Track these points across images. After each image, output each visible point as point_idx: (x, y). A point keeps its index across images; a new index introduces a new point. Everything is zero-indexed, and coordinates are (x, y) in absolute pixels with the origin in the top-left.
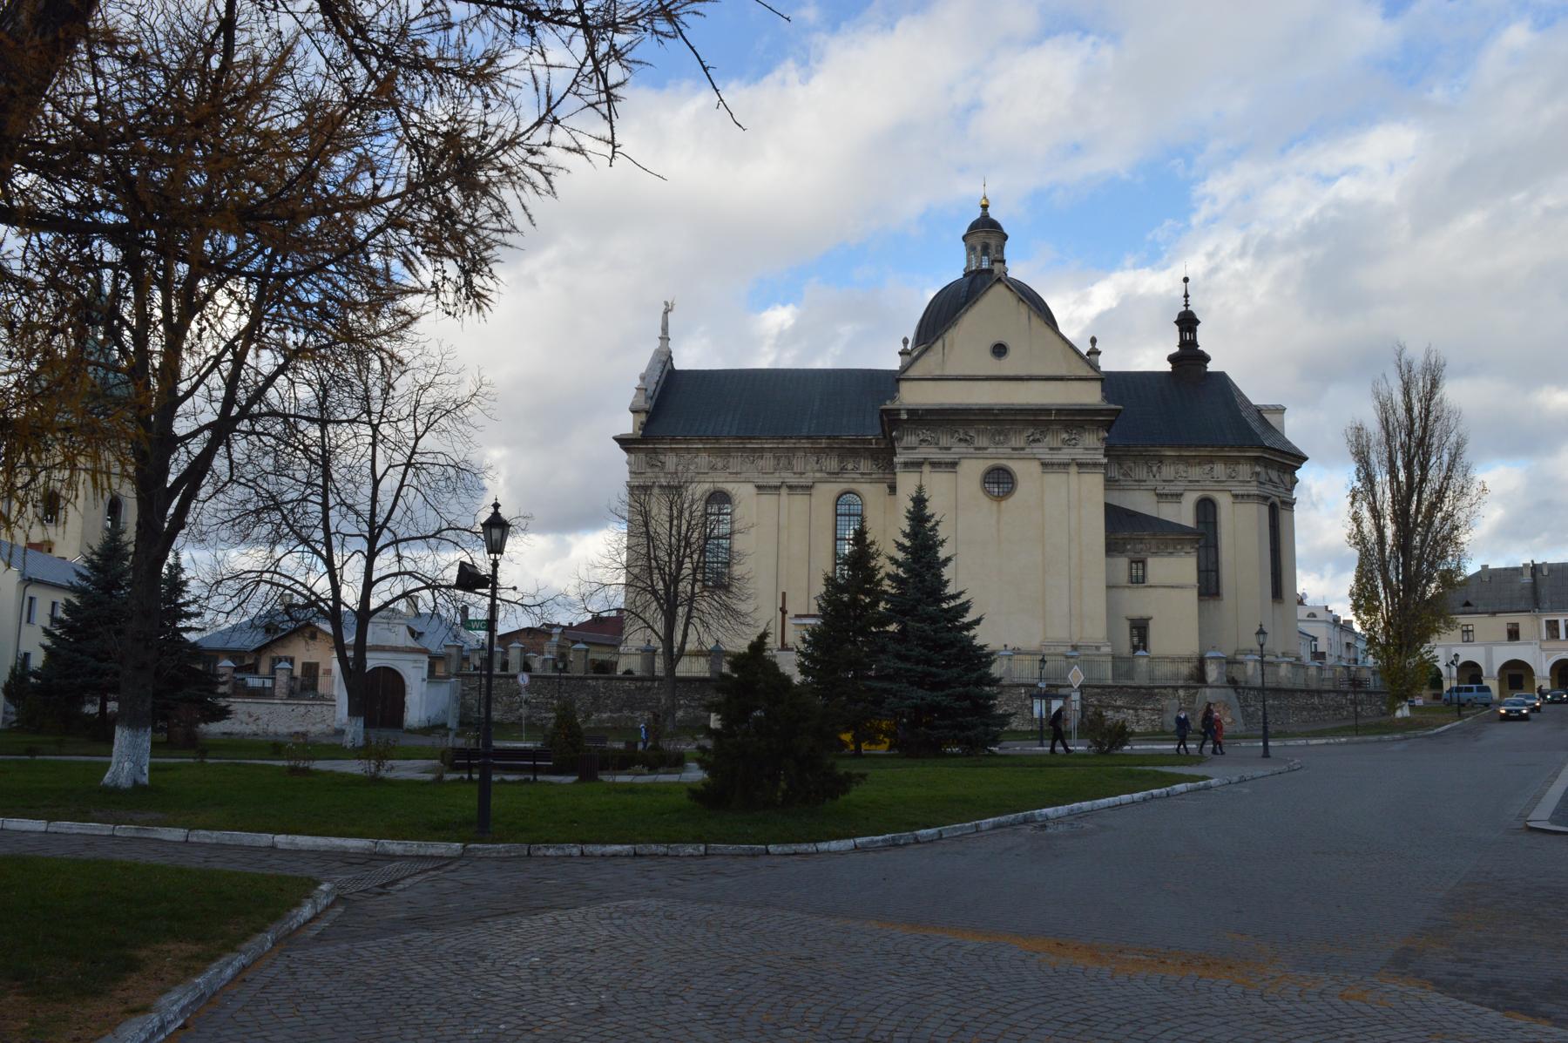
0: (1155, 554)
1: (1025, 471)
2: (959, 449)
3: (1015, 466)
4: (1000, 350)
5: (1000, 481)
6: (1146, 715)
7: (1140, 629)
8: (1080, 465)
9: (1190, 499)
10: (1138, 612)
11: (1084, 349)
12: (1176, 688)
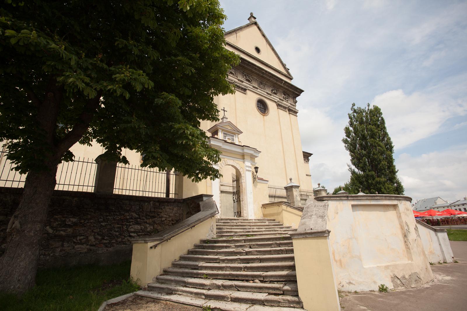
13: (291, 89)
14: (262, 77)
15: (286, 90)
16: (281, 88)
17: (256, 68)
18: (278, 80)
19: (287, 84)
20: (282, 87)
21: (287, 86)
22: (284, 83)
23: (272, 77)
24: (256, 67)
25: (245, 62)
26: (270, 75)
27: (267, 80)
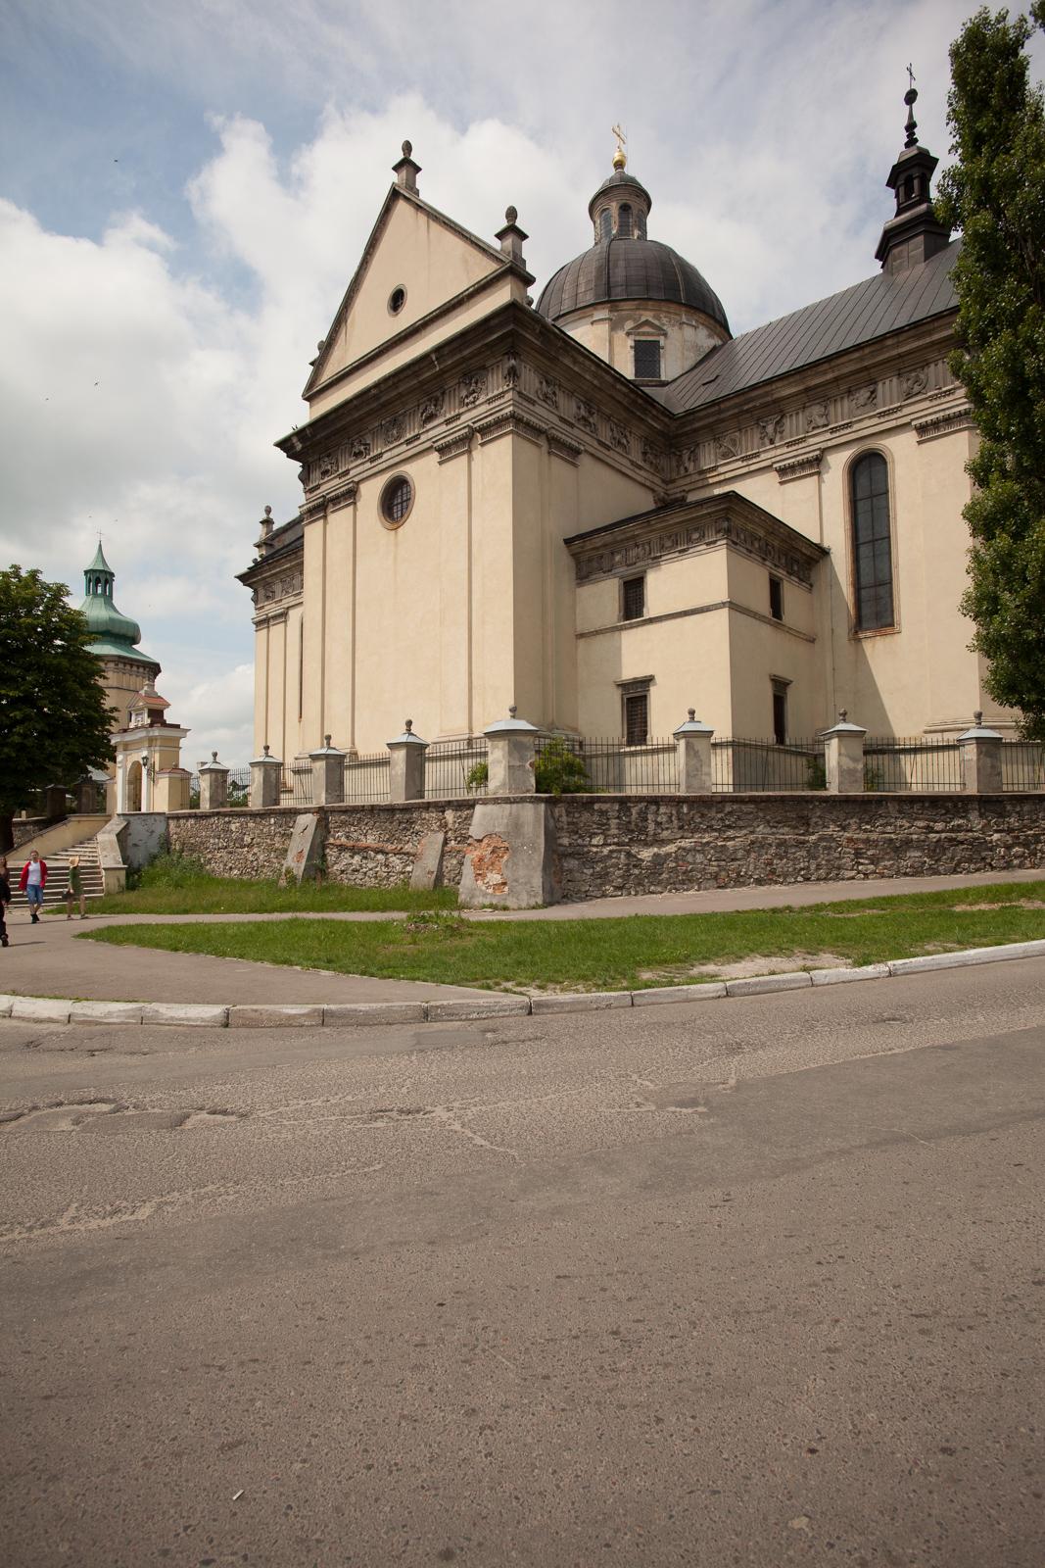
0: (656, 561)
1: (423, 473)
2: (357, 468)
3: (410, 470)
4: (397, 299)
5: (396, 500)
6: (394, 860)
7: (635, 698)
8: (484, 430)
9: (838, 463)
10: (630, 671)
11: (487, 227)
12: (441, 807)
13: (468, 347)
14: (383, 405)
15: (464, 365)
16: (445, 376)
17: (356, 406)
18: (416, 368)
19: (446, 350)
20: (443, 372)
21: (452, 353)
22: (437, 359)
23: (400, 381)
24: (355, 402)
25: (330, 418)
26: (390, 382)
27: (399, 402)
